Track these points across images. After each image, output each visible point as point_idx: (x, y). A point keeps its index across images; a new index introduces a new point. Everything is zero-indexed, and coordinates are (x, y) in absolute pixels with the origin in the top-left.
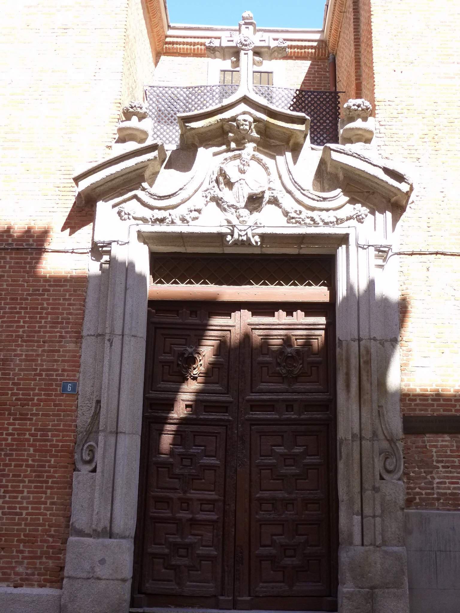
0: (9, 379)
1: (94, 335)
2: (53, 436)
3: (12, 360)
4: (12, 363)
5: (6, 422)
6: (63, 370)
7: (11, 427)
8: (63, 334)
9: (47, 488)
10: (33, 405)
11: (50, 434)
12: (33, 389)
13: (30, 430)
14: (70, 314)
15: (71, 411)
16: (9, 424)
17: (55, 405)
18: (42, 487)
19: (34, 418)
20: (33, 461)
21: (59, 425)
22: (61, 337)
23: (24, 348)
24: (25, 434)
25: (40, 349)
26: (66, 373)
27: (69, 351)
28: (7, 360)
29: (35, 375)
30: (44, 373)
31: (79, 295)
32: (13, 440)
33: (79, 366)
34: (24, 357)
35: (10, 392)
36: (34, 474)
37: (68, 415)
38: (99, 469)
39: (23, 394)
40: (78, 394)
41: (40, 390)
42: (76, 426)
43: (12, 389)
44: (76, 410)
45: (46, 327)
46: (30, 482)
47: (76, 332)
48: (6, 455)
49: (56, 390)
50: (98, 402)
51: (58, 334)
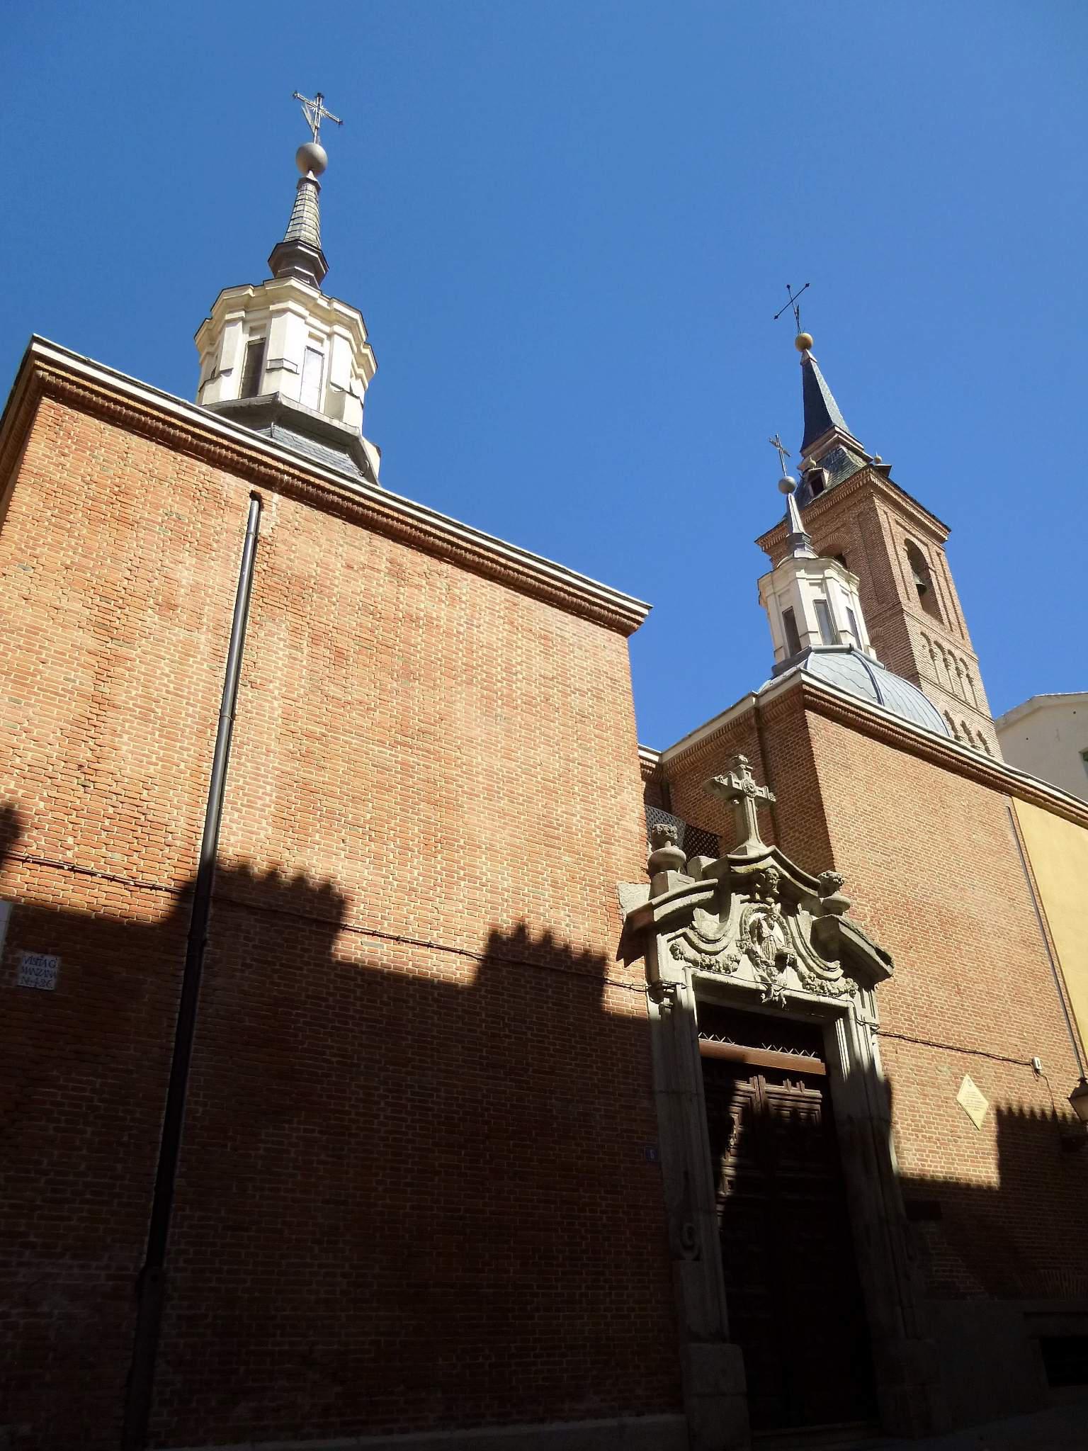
50: (686, 1173)
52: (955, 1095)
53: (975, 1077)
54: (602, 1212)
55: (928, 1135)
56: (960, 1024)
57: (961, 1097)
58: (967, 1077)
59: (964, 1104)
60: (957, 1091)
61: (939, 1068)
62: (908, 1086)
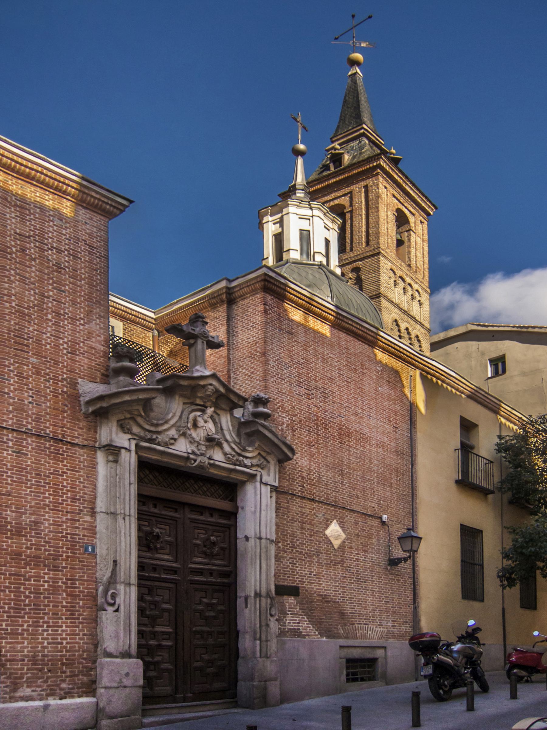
0: (41, 538)
1: (105, 513)
2: (79, 584)
3: (42, 523)
4: (42, 526)
5: (42, 572)
6: (84, 536)
7: (46, 576)
8: (81, 508)
9: (80, 623)
10: (63, 560)
11: (77, 583)
12: (62, 548)
13: (62, 579)
14: (86, 494)
15: (92, 566)
16: (45, 574)
17: (80, 561)
18: (75, 623)
19: (64, 570)
20: (67, 603)
21: (84, 576)
22: (80, 510)
23: (51, 515)
24: (58, 582)
25: (65, 518)
26: (86, 538)
27: (87, 522)
28: (38, 523)
29: (62, 537)
30: (69, 536)
31: (91, 481)
32: (49, 586)
33: (95, 534)
34: (51, 522)
35: (43, 548)
36: (68, 613)
37: (90, 570)
38: (122, 608)
39: (54, 551)
40: (96, 555)
41: (67, 548)
42: (96, 578)
43: (45, 546)
44: (96, 566)
45: (67, 501)
46: (66, 619)
47: (91, 508)
48: (45, 598)
49: (80, 550)
51: (77, 508)
52: (324, 530)
53: (340, 522)
54: (44, 582)
55: (300, 550)
56: (338, 492)
57: (328, 532)
58: (335, 521)
59: (329, 535)
60: (326, 528)
61: (317, 514)
62: (292, 523)
